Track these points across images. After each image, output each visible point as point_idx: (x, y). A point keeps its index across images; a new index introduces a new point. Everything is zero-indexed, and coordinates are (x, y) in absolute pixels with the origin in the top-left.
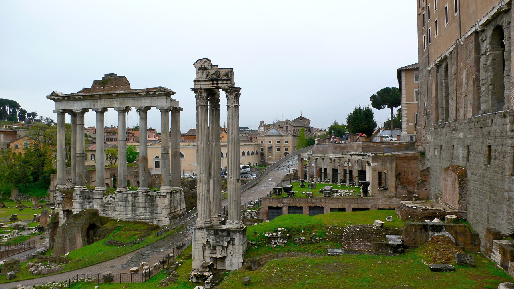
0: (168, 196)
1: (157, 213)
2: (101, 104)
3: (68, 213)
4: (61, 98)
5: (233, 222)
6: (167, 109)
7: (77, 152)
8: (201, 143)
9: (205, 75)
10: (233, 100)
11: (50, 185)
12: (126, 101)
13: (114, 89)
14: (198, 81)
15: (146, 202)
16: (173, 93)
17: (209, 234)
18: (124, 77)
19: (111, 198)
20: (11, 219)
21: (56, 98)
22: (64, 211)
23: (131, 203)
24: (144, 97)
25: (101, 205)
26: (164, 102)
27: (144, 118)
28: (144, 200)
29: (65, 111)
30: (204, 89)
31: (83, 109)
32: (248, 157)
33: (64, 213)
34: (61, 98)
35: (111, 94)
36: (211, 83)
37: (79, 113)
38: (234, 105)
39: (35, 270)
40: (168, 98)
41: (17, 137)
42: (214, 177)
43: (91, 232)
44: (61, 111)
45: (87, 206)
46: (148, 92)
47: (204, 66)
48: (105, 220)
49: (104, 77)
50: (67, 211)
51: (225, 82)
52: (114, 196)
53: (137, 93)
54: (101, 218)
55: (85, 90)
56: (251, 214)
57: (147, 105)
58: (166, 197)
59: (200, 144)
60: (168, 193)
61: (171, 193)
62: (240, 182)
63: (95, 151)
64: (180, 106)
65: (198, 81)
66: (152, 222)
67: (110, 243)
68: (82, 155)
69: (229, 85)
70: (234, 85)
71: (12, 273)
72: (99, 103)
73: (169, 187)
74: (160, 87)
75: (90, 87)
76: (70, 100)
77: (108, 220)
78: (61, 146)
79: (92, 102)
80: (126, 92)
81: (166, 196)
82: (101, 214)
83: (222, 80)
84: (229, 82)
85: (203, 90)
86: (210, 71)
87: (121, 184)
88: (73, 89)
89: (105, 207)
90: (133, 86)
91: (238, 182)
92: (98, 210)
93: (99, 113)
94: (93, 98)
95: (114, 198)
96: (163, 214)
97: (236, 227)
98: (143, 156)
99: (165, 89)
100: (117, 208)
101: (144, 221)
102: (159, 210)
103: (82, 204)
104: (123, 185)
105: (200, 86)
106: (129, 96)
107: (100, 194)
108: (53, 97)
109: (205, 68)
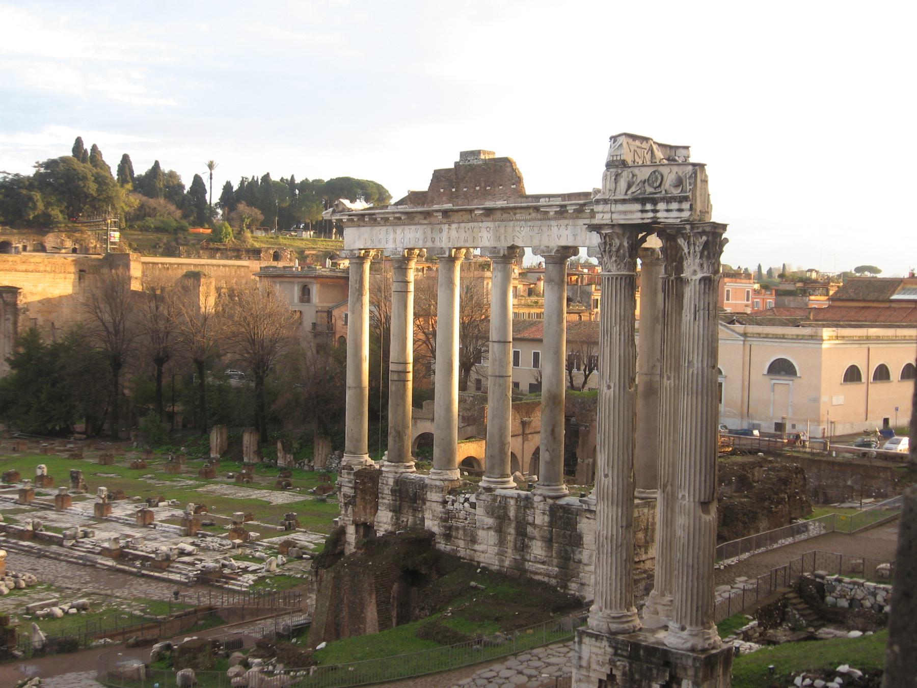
3: (366, 529)
5: (683, 629)
8: (609, 387)
9: (623, 184)
10: (698, 260)
12: (510, 230)
13: (485, 195)
15: (551, 524)
17: (616, 654)
19: (466, 505)
22: (357, 526)
23: (513, 525)
24: (555, 219)
28: (547, 519)
33: (357, 532)
36: (638, 207)
38: (700, 275)
39: (237, 675)
45: (408, 519)
46: (565, 206)
49: (458, 159)
50: (365, 524)
51: (674, 206)
52: (473, 498)
54: (440, 555)
55: (415, 197)
56: (874, 595)
57: (563, 243)
59: (605, 389)
66: (565, 587)
67: (426, 635)
69: (686, 215)
70: (707, 211)
71: (189, 671)
72: (444, 235)
75: (426, 189)
76: (379, 224)
77: (453, 559)
79: (428, 230)
82: (442, 545)
83: (669, 200)
84: (686, 206)
85: (618, 231)
86: (636, 171)
89: (450, 528)
90: (531, 187)
92: (433, 534)
94: (433, 220)
95: (473, 506)
97: (689, 645)
98: (549, 391)
100: (481, 534)
101: (546, 579)
103: (397, 510)
104: (497, 471)
105: (608, 216)
106: (518, 216)
107: (441, 489)
109: (624, 164)
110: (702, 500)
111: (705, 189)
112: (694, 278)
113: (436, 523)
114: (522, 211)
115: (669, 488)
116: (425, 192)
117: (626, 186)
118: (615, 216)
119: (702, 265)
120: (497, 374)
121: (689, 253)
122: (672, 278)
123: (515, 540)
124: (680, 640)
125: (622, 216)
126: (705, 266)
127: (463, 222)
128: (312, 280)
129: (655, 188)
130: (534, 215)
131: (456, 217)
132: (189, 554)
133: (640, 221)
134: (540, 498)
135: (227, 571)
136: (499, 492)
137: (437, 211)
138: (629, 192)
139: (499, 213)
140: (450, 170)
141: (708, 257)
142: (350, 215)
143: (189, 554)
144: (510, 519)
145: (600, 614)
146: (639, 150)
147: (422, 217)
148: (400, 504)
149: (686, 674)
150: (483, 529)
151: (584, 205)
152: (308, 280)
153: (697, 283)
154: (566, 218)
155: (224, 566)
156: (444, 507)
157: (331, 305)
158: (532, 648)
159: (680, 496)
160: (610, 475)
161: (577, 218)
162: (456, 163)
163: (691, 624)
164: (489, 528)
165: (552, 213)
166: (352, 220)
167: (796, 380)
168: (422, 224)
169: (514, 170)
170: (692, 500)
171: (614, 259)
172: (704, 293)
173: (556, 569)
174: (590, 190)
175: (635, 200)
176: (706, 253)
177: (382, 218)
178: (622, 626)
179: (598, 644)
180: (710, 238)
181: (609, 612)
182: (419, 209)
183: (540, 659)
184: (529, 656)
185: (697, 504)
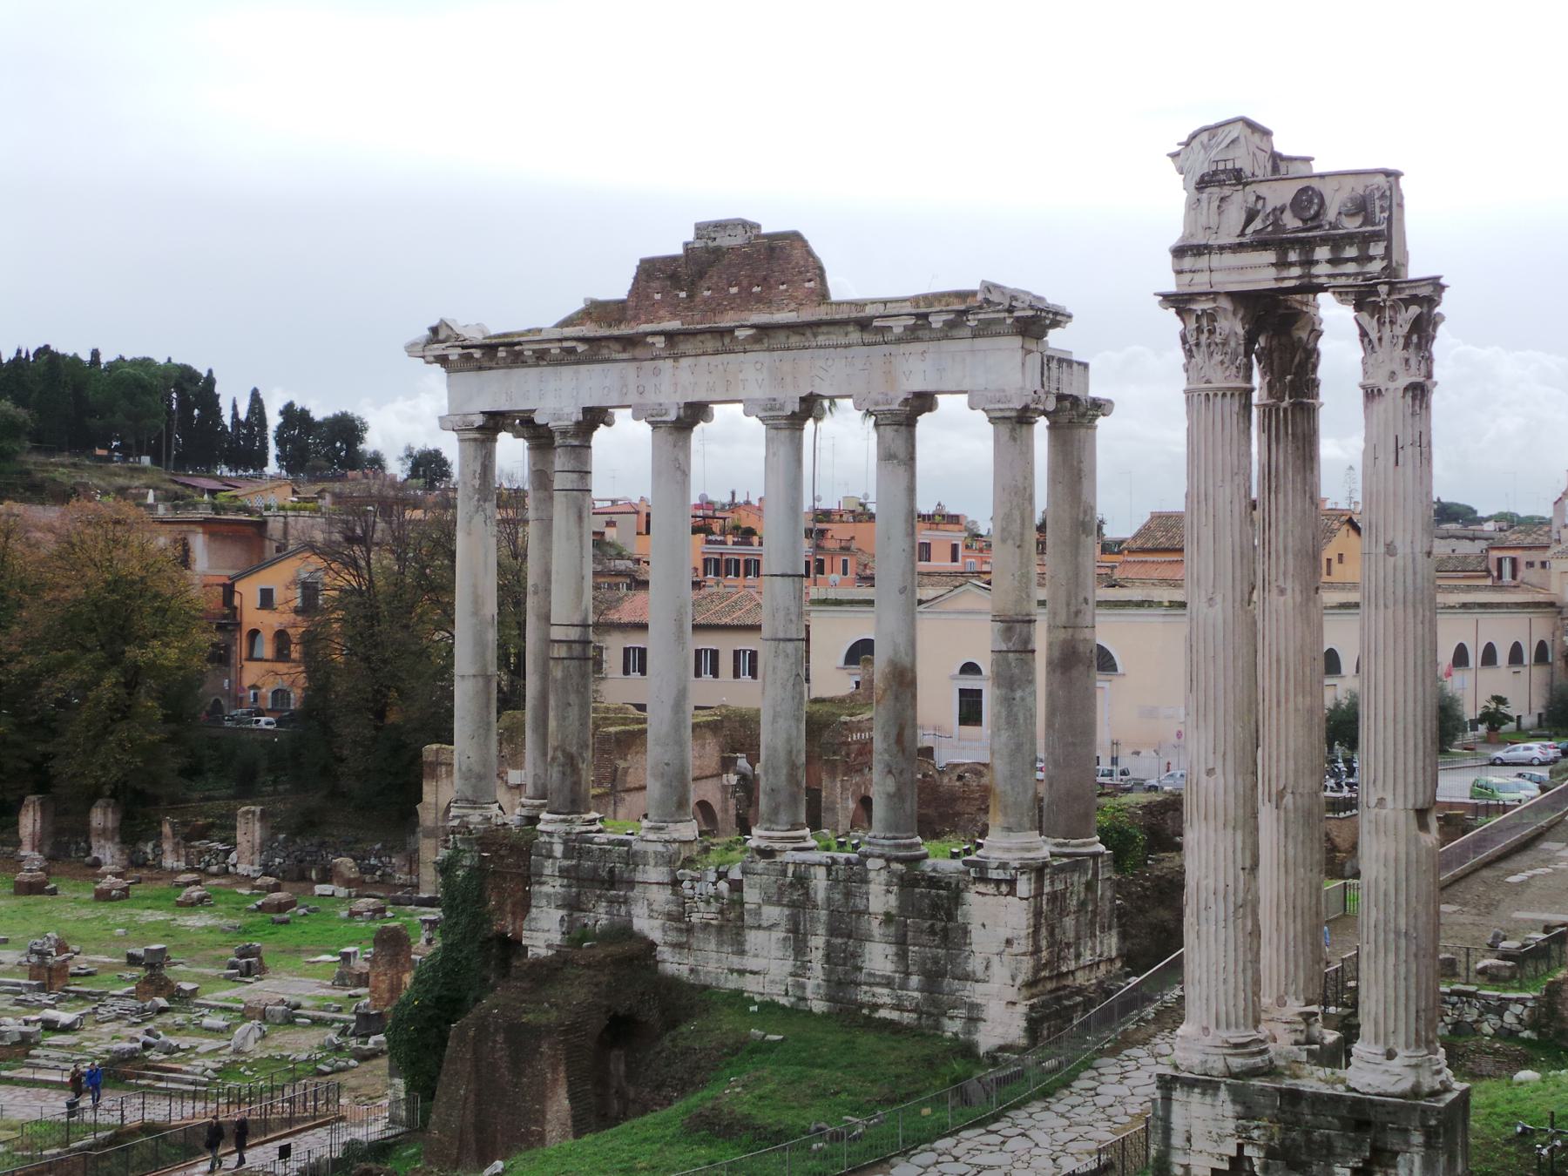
0: (1024, 886)
1: (967, 977)
2: (676, 382)
4: (477, 354)
5: (1390, 1055)
6: (1026, 408)
7: (557, 633)
9: (1234, 216)
10: (1399, 353)
11: (420, 800)
13: (747, 300)
14: (1199, 250)
16: (1057, 318)
18: (795, 238)
20: (233, 966)
21: (454, 354)
23: (823, 914)
24: (899, 340)
25: (670, 916)
26: (1007, 368)
27: (902, 454)
29: (495, 422)
30: (1230, 294)
31: (586, 410)
32: (1487, 674)
34: (477, 354)
35: (731, 331)
36: (1270, 256)
37: (564, 433)
38: (1403, 380)
40: (1031, 344)
41: (270, 549)
42: (1281, 795)
43: (618, 1064)
44: (479, 421)
45: (599, 916)
46: (925, 316)
47: (1229, 166)
48: (683, 1000)
51: (1351, 252)
53: (864, 324)
54: (674, 983)
55: (597, 311)
58: (1012, 892)
60: (1024, 868)
61: (1039, 871)
62: (1434, 825)
63: (643, 627)
64: (1096, 391)
65: (1199, 250)
68: (577, 649)
73: (1034, 837)
74: (989, 287)
76: (524, 364)
78: (477, 602)
79: (630, 368)
80: (807, 315)
81: (1012, 883)
82: (673, 964)
85: (1225, 303)
87: (775, 811)
88: (541, 307)
90: (845, 284)
91: (1423, 826)
92: (653, 945)
93: (662, 431)
94: (639, 352)
96: (994, 986)
97: (1406, 1085)
99: (1014, 298)
102: (975, 965)
103: (572, 905)
104: (784, 817)
106: (821, 340)
107: (669, 861)
108: (438, 349)
109: (1238, 178)
110: (1419, 806)
111: (1401, 220)
112: (1392, 385)
113: (658, 923)
114: (831, 329)
115: (1288, 799)
116: (622, 302)
117: (1243, 217)
118: (1217, 277)
119: (1407, 361)
120: (781, 635)
121: (1380, 339)
122: (1287, 402)
123: (828, 943)
124: (1386, 1077)
125: (1235, 276)
126: (1413, 362)
127: (704, 354)
128: (192, 527)
129: (1305, 221)
130: (855, 336)
131: (687, 346)
132: (68, 1029)
133: (1273, 285)
134: (881, 862)
135: (154, 1056)
136: (790, 856)
137: (654, 334)
138: (1249, 230)
139: (781, 337)
140: (674, 259)
141: (1419, 347)
142: (463, 347)
143: (68, 1029)
144: (815, 907)
145: (1208, 1040)
146: (1258, 152)
147: (617, 347)
148: (579, 894)
149: (1408, 1143)
150: (759, 927)
151: (965, 312)
152: (185, 527)
153: (1400, 393)
154: (918, 339)
155: (147, 1046)
156: (675, 893)
157: (231, 573)
158: (932, 1142)
159: (1373, 801)
160: (1219, 771)
161: (947, 337)
162: (686, 244)
163: (1407, 1047)
164: (770, 928)
165: (898, 330)
166: (469, 357)
167: (1115, 678)
168: (607, 361)
169: (809, 253)
170: (1401, 806)
171: (1218, 358)
172: (1413, 414)
173: (916, 994)
174: (976, 286)
175: (1261, 244)
176: (1415, 338)
177: (534, 351)
178: (1251, 1061)
179: (1208, 1100)
180: (1425, 310)
181: (1224, 1034)
182: (615, 332)
183: (957, 1159)
184: (928, 1158)
185: (1412, 813)
